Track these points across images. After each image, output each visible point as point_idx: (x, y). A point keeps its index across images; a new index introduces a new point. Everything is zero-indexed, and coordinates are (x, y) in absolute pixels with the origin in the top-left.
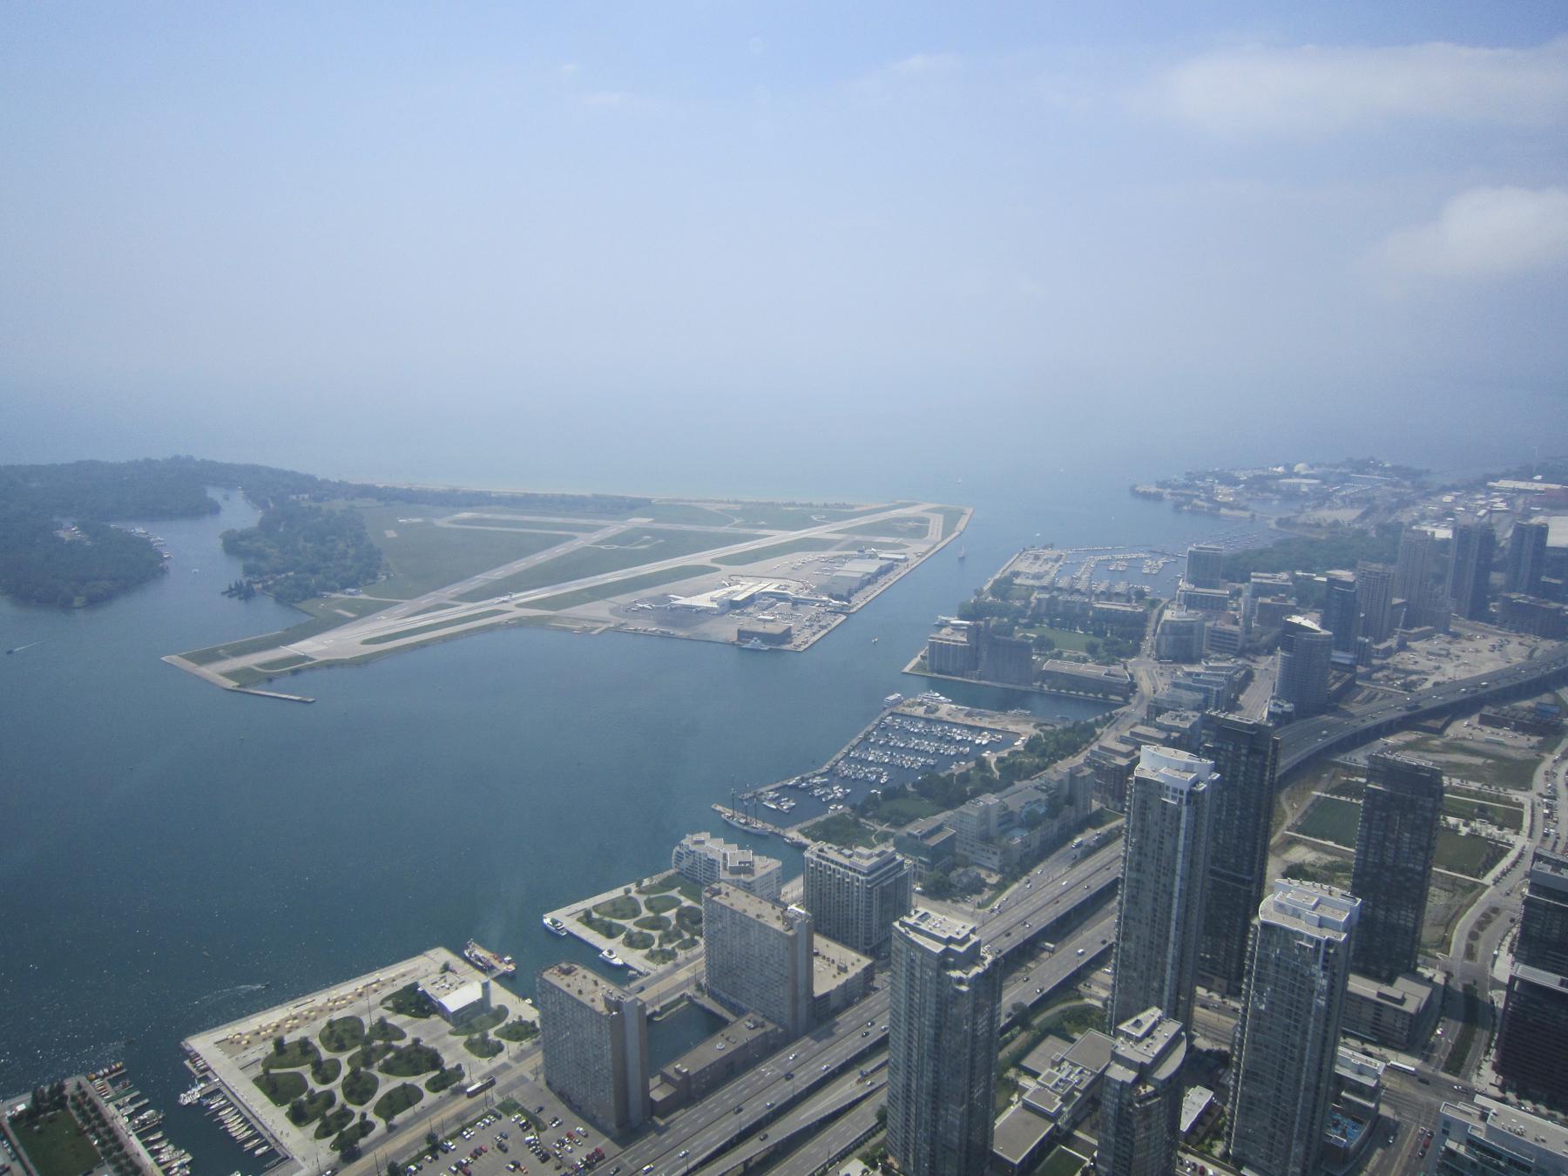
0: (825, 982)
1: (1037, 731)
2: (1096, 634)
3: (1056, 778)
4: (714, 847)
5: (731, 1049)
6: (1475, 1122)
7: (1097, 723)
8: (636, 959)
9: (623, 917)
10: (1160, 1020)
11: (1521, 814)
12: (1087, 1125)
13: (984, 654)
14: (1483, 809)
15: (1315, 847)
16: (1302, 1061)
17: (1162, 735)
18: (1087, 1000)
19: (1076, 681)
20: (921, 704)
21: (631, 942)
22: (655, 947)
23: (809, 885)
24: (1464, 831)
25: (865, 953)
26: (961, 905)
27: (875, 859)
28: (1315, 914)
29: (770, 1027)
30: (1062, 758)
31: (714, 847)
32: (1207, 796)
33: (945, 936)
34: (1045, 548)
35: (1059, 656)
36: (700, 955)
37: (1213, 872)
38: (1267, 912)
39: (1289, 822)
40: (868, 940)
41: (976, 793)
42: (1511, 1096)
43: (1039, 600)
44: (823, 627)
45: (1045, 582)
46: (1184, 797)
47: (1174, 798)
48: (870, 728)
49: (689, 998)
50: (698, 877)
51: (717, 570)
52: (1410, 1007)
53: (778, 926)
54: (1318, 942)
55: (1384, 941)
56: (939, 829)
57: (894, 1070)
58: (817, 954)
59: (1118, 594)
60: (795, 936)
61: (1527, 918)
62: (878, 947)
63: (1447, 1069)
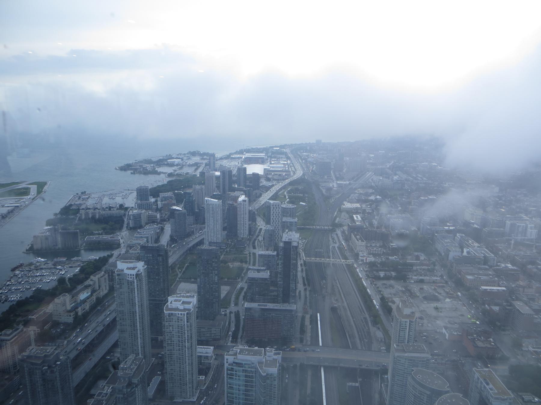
11: (246, 257)
19: (99, 242)
32: (143, 274)
35: (92, 234)
39: (179, 276)
41: (60, 294)
43: (81, 214)
45: (83, 207)
46: (135, 276)
47: (131, 278)
54: (184, 314)
59: (113, 208)
63: (232, 342)
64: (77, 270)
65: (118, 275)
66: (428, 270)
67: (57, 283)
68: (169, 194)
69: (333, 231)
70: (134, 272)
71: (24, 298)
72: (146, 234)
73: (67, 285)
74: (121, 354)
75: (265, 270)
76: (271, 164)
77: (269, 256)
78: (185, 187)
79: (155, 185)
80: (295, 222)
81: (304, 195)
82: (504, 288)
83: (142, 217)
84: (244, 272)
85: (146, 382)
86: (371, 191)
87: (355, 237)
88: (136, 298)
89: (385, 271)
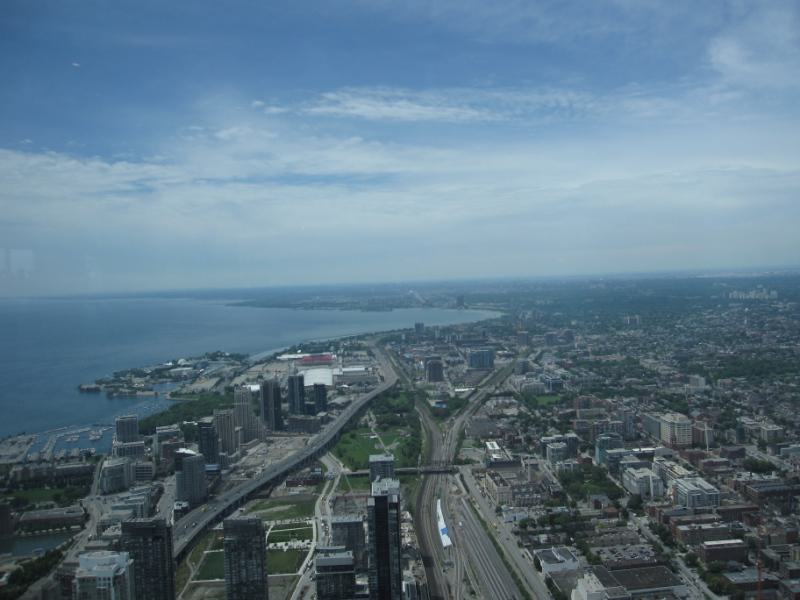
1: (18, 566)
2: (59, 487)
7: (64, 548)
11: (311, 530)
14: (293, 533)
15: (208, 585)
17: (106, 544)
24: (285, 548)
30: (38, 579)
32: (127, 576)
35: (32, 508)
39: (192, 575)
43: (15, 472)
46: (111, 582)
47: (105, 585)
59: (73, 457)
65: (82, 580)
66: (619, 525)
72: (131, 502)
75: (346, 550)
79: (148, 415)
82: (739, 541)
83: (125, 470)
89: (550, 532)
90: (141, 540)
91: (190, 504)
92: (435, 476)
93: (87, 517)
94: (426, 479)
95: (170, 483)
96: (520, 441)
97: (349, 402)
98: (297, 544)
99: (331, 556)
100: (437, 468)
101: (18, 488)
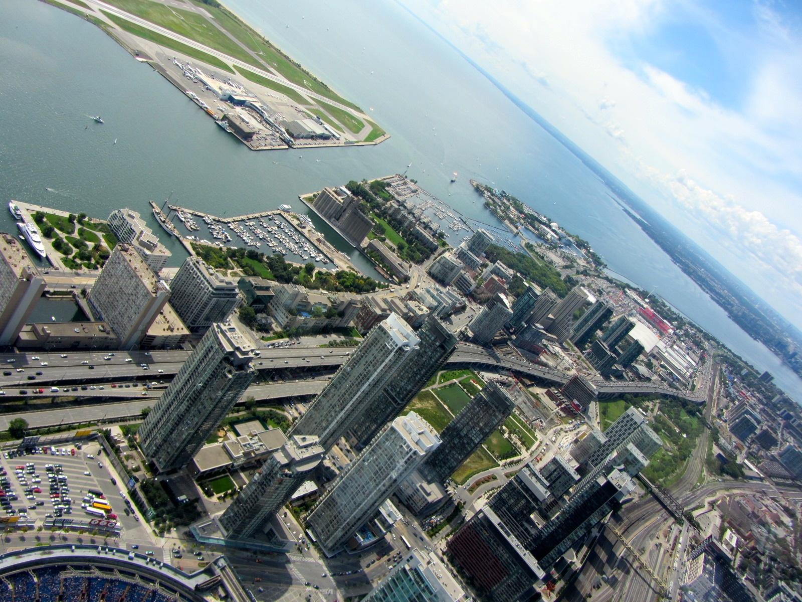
0: (157, 330)
1: (347, 270)
2: (407, 241)
3: (342, 300)
4: (139, 224)
5: (82, 335)
6: (425, 566)
7: (379, 286)
8: (56, 257)
9: (61, 229)
10: (315, 444)
11: (533, 443)
12: (247, 473)
13: (347, 215)
14: (520, 431)
16: (367, 497)
17: (405, 311)
18: (286, 414)
19: (382, 259)
20: (298, 219)
21: (58, 246)
22: (71, 257)
23: (178, 276)
24: (506, 435)
25: (188, 327)
26: (254, 333)
27: (224, 284)
28: (418, 437)
29: (112, 336)
31: (139, 224)
32: (407, 354)
33: (237, 346)
34: (412, 181)
35: (383, 240)
36: (95, 276)
37: (385, 390)
38: (398, 423)
39: (436, 386)
40: (194, 321)
41: (297, 283)
42: (445, 558)
43: (392, 206)
44: (271, 145)
45: (400, 199)
46: (396, 348)
47: (391, 346)
48: (264, 214)
49: (74, 295)
50: (117, 234)
51: (234, 73)
52: (430, 499)
53: (150, 287)
54: (411, 450)
55: (439, 465)
56: (267, 288)
57: (167, 395)
58: (162, 313)
59: (431, 229)
60: (156, 298)
61: (505, 490)
62: (197, 330)
64: (334, 271)
67: (304, 266)
68: (510, 272)
69: (679, 521)
70: (401, 341)
71: (259, 252)
72: (441, 297)
73: (312, 277)
74: (302, 417)
75: (548, 488)
76: (671, 347)
77: (564, 472)
78: (533, 280)
80: (642, 465)
81: (680, 432)
84: (515, 459)
85: (301, 478)
86: (786, 519)
87: (706, 561)
88: (376, 373)
90: (433, 338)
91: (474, 337)
92: (659, 507)
93: (406, 279)
94: (649, 501)
95: (476, 310)
96: (759, 561)
97: (649, 380)
98: (515, 439)
99: (534, 480)
100: (667, 502)
101: (385, 217)
